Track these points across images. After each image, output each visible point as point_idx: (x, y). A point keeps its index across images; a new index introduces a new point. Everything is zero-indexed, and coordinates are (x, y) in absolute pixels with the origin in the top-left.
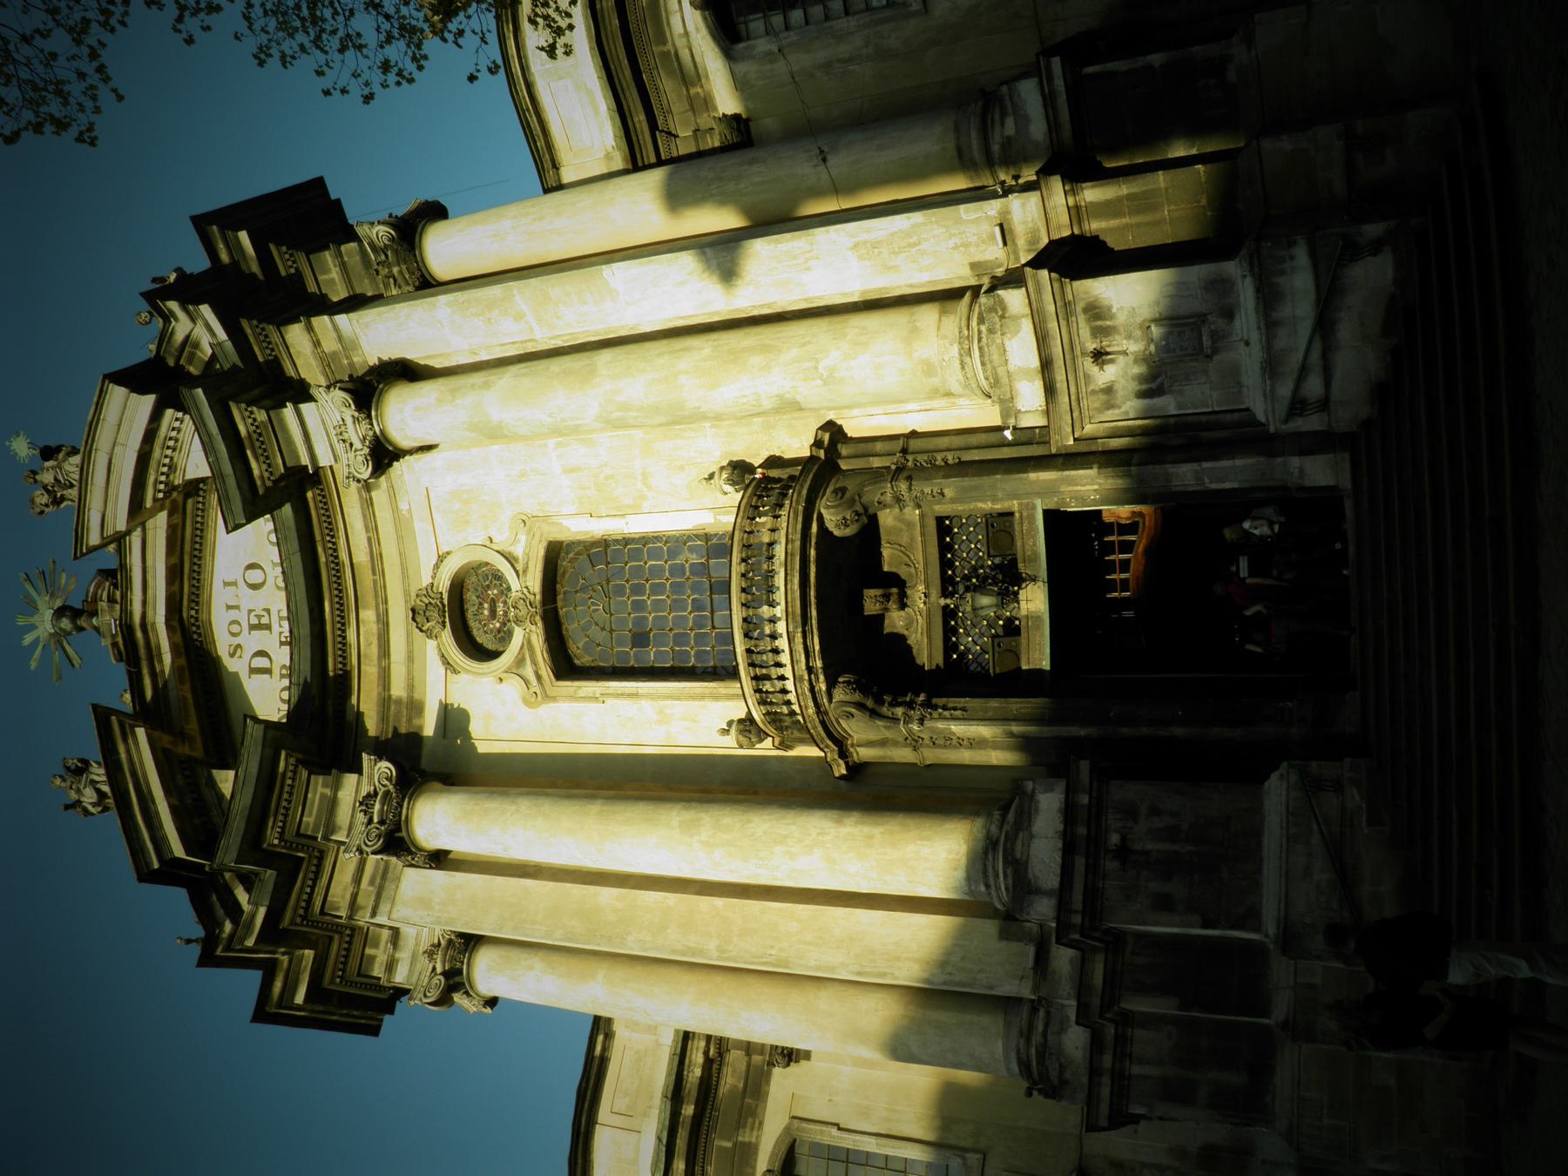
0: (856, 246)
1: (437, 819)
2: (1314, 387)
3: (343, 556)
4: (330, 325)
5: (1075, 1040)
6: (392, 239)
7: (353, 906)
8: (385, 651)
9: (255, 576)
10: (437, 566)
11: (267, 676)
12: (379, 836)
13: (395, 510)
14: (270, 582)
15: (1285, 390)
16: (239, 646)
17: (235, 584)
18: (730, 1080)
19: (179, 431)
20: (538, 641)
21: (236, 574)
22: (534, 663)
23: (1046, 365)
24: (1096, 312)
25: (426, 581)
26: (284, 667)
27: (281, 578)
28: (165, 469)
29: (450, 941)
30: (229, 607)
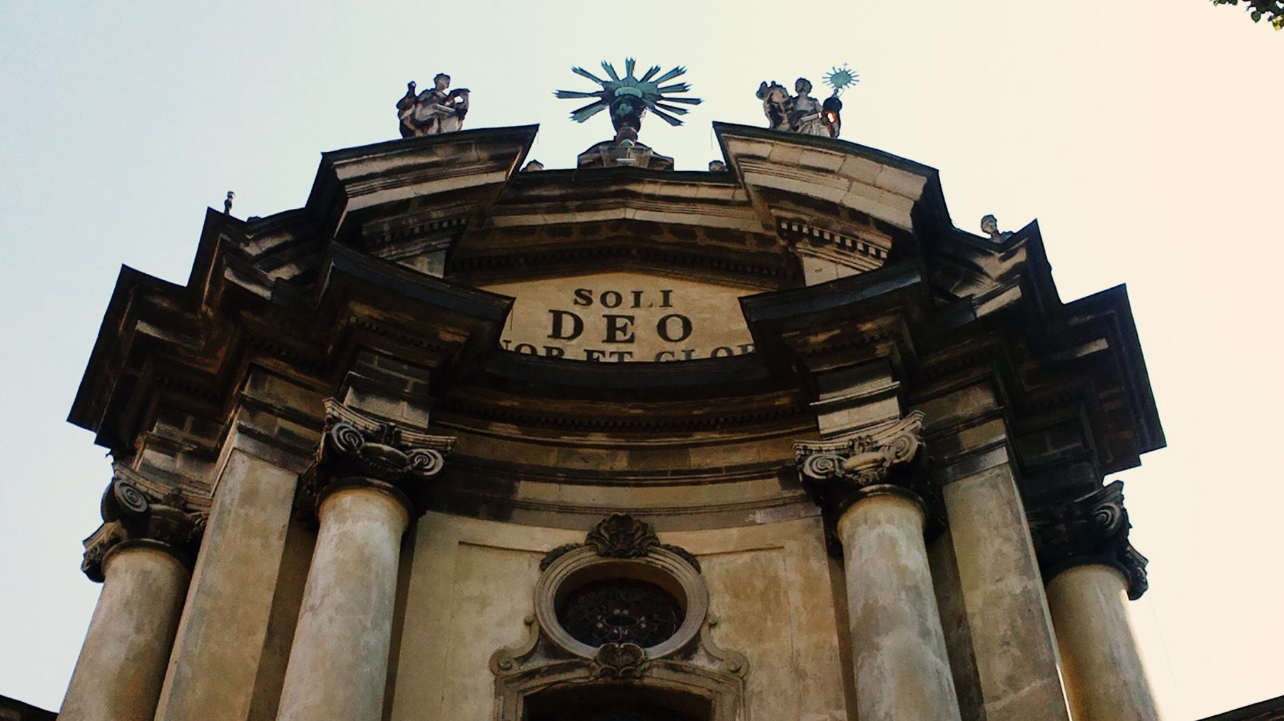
1: (361, 525)
3: (698, 437)
4: (994, 440)
6: (1103, 526)
7: (254, 407)
8: (576, 478)
9: (675, 329)
10: (680, 552)
11: (550, 332)
12: (349, 446)
13: (754, 506)
14: (668, 346)
16: (589, 302)
17: (666, 303)
19: (865, 252)
21: (677, 306)
22: (551, 670)
25: (666, 537)
26: (561, 351)
27: (671, 358)
28: (816, 234)
29: (190, 524)
30: (637, 295)
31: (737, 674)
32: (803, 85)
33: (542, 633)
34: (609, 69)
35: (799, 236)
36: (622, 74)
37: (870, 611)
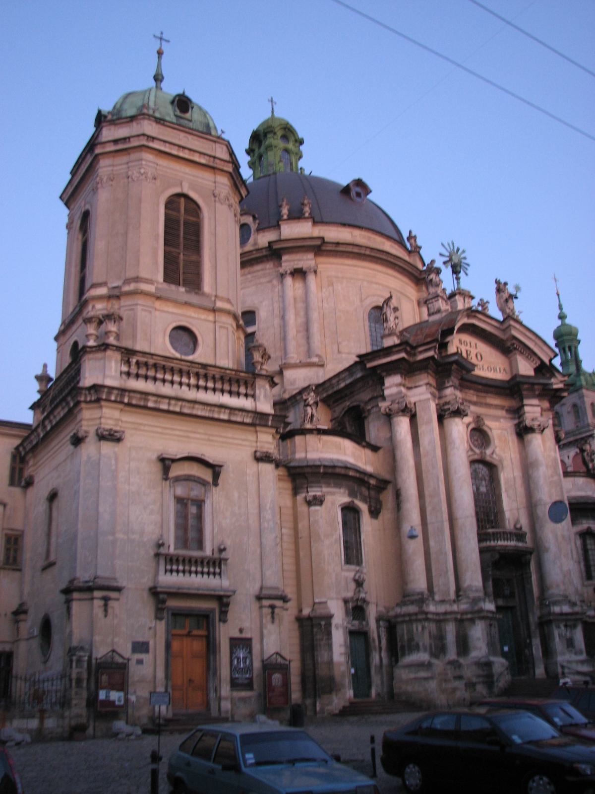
0: (569, 570)
2: (566, 671)
5: (432, 608)
15: (565, 664)
16: (462, 344)
18: (365, 491)
20: (476, 457)
21: (478, 350)
23: (567, 614)
24: (575, 626)
28: (522, 351)
31: (501, 461)
32: (506, 284)
33: (470, 445)
34: (449, 244)
35: (518, 350)
36: (452, 249)
37: (537, 460)
